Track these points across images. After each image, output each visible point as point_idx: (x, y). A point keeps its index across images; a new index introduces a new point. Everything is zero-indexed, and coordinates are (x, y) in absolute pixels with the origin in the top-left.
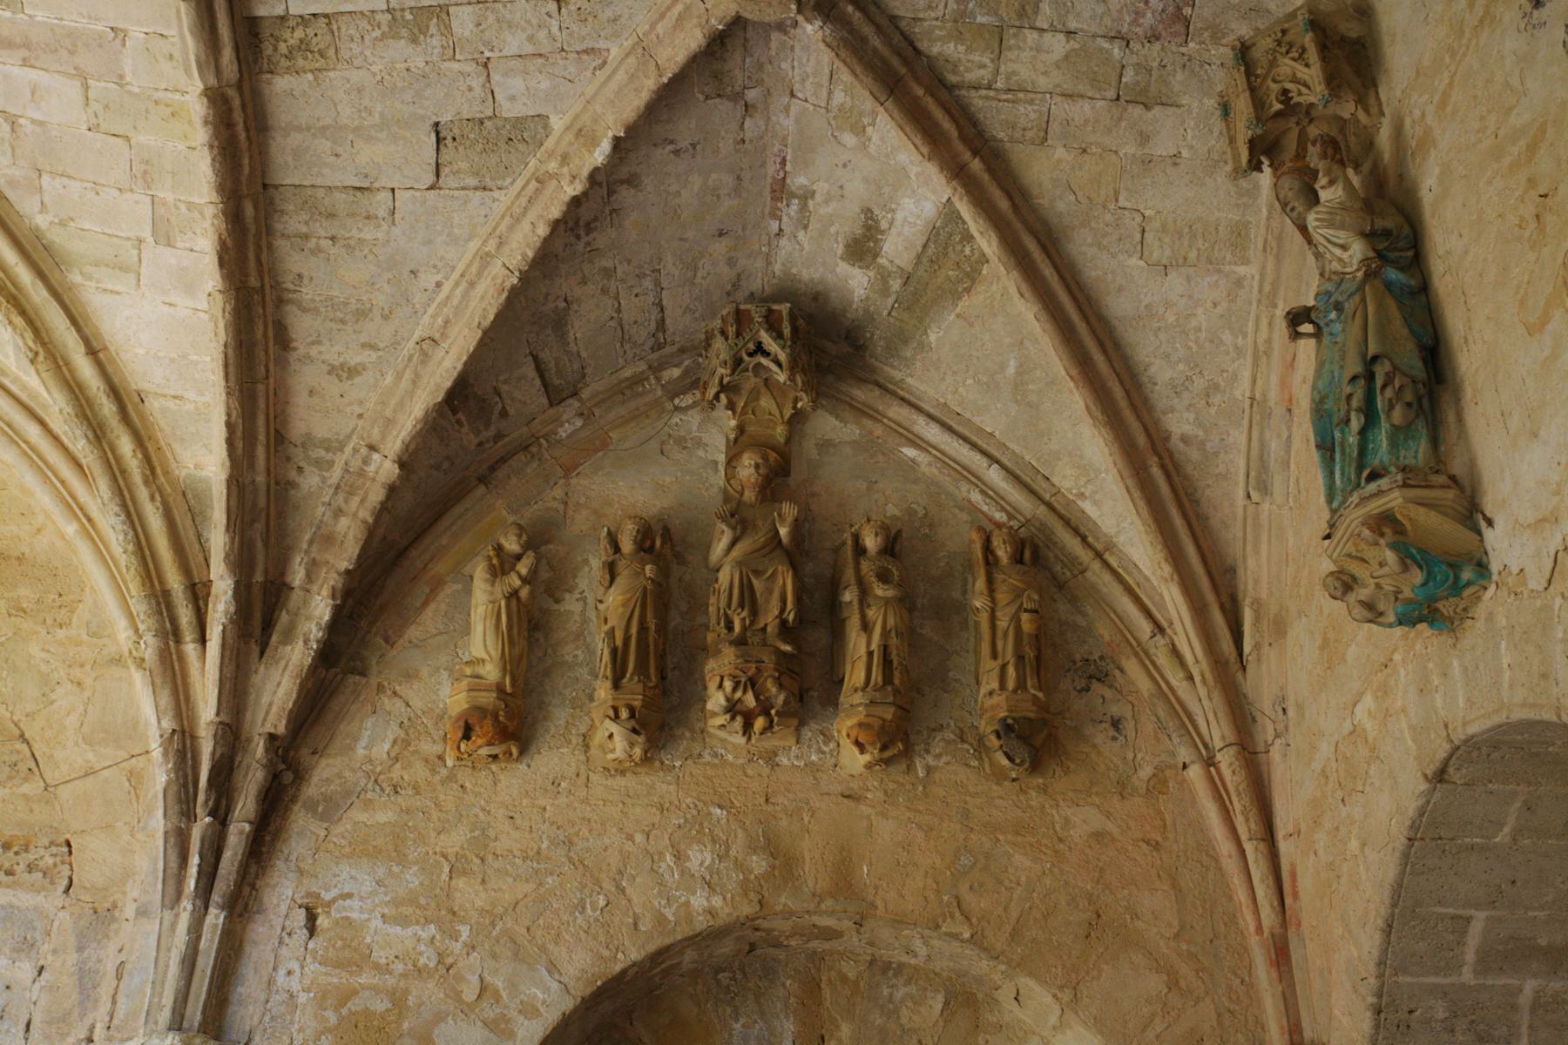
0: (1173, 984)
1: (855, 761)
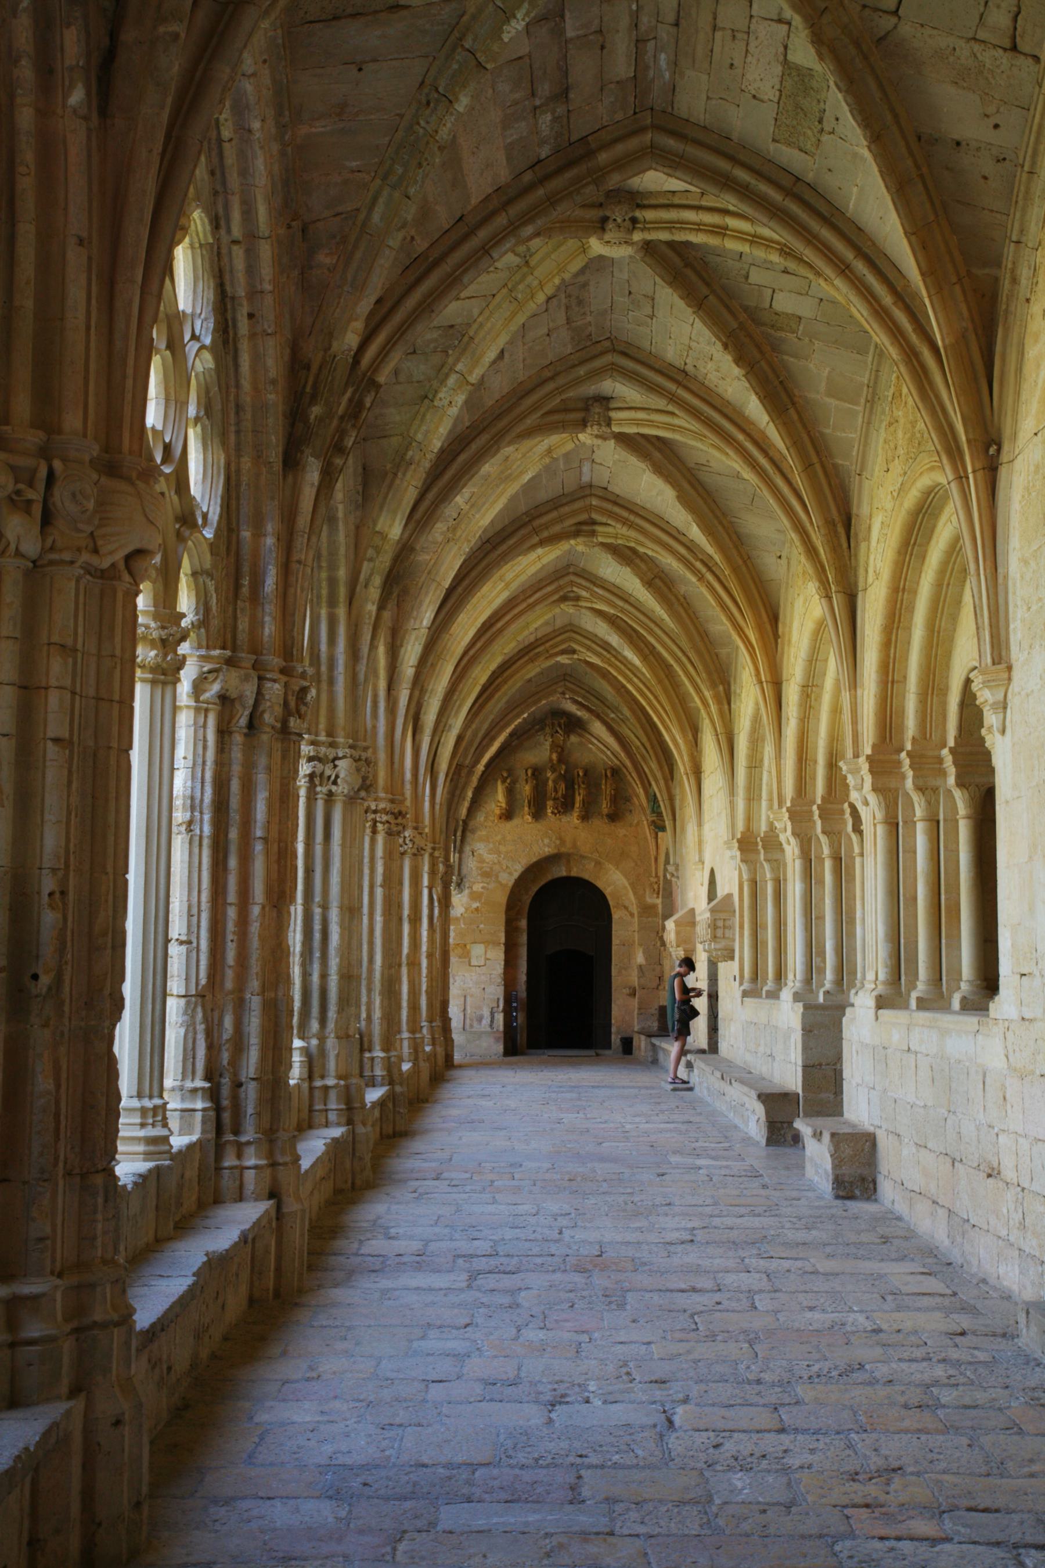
0: (636, 865)
1: (576, 821)
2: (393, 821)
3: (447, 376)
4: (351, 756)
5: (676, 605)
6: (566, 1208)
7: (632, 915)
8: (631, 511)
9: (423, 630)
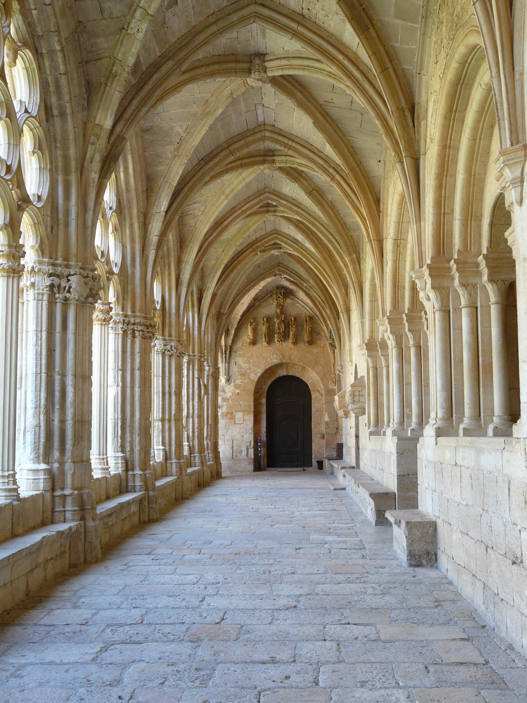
2: (145, 330)
3: (135, 11)
4: (80, 274)
5: (326, 206)
6: (220, 579)
7: (322, 395)
8: (289, 139)
9: (161, 213)
